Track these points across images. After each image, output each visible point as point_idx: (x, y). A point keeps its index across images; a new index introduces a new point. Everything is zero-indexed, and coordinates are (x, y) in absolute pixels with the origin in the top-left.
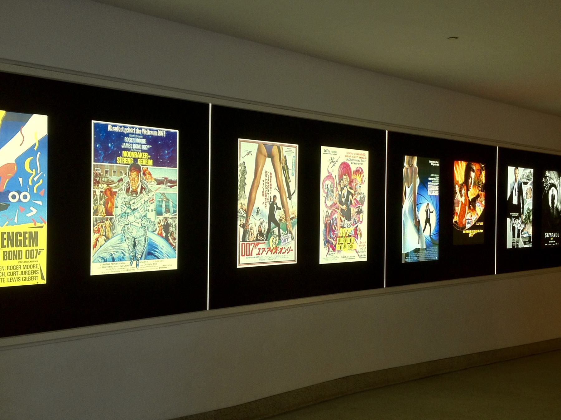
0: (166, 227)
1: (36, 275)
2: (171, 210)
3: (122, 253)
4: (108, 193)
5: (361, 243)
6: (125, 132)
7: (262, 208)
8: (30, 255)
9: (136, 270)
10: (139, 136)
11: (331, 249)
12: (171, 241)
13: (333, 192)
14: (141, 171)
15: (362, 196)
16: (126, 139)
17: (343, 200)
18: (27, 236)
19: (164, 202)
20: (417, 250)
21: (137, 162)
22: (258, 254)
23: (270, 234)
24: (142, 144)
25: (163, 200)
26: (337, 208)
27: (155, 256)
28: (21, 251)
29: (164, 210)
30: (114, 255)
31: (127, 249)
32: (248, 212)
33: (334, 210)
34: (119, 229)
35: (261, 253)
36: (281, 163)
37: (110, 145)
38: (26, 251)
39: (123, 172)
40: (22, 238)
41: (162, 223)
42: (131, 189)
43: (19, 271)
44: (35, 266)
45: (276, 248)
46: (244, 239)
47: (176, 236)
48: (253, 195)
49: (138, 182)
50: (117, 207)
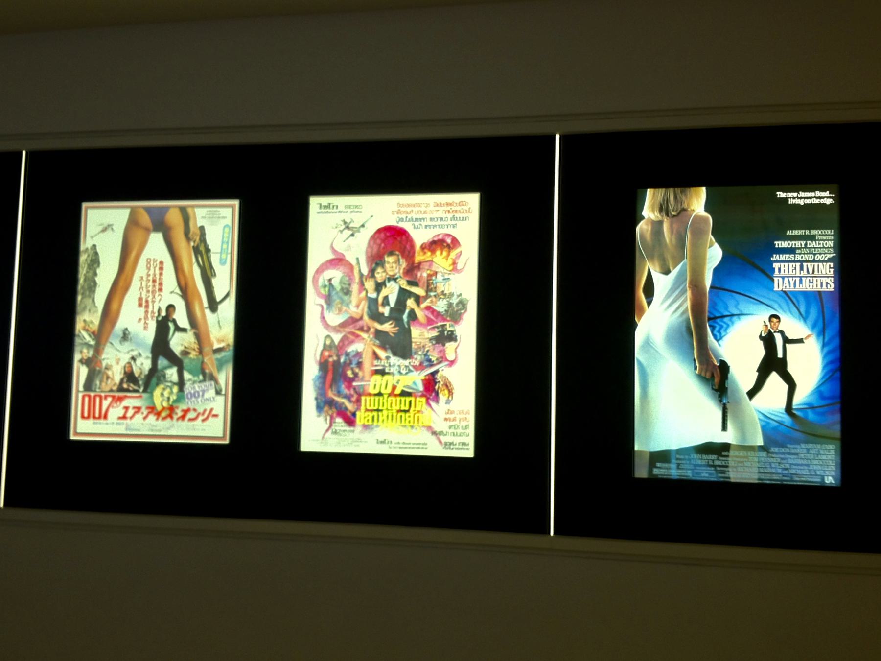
5: (449, 412)
7: (135, 328)
11: (339, 420)
13: (347, 292)
15: (455, 300)
17: (386, 311)
20: (714, 450)
22: (124, 417)
23: (154, 380)
26: (361, 329)
32: (101, 336)
33: (353, 334)
35: (129, 414)
36: (188, 239)
45: (172, 409)
46: (88, 386)
48: (114, 306)
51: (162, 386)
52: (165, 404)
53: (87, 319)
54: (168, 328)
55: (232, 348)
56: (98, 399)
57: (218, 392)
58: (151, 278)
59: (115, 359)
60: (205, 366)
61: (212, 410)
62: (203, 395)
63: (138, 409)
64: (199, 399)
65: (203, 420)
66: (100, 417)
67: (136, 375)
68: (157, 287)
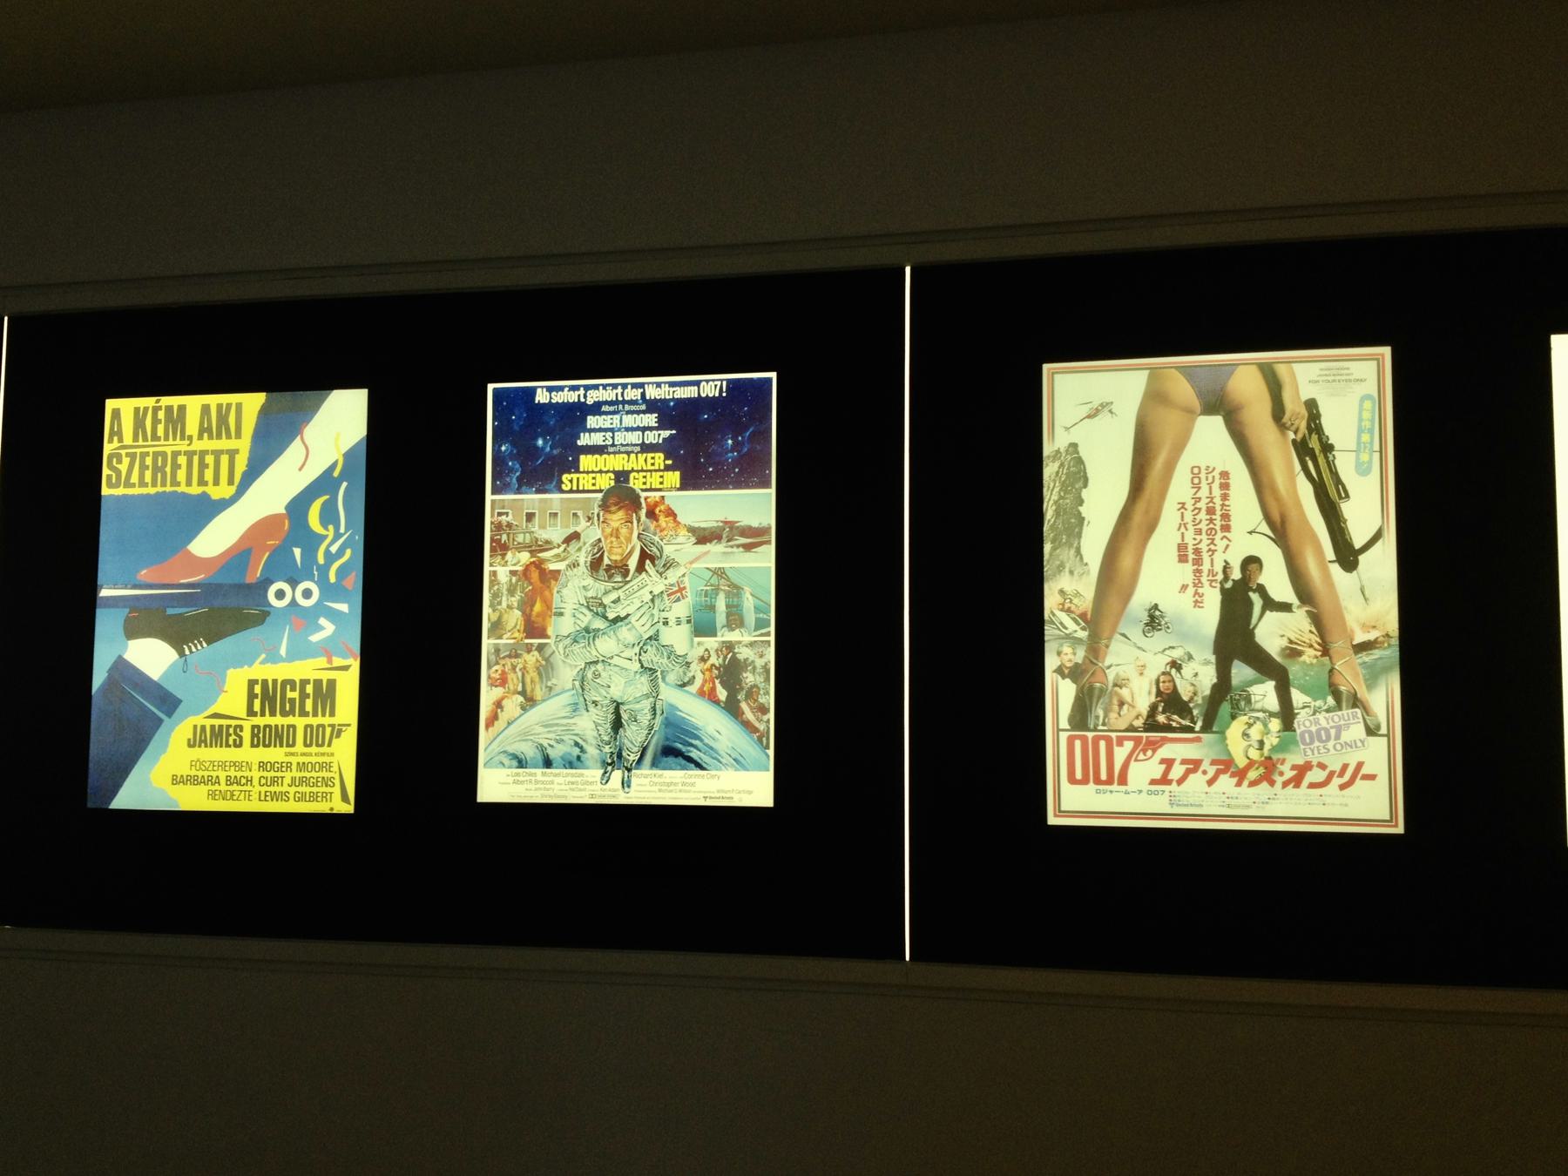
0: (731, 672)
1: (328, 790)
2: (750, 618)
3: (577, 744)
4: (535, 575)
6: (590, 401)
7: (1174, 603)
8: (315, 737)
9: (622, 798)
10: (633, 408)
12: (749, 715)
14: (637, 506)
16: (592, 421)
18: (309, 689)
19: (722, 596)
21: (627, 480)
22: (1164, 780)
23: (1225, 708)
24: (644, 429)
25: (717, 590)
27: (690, 760)
28: (294, 727)
29: (721, 618)
30: (550, 751)
31: (590, 734)
34: (566, 675)
37: (540, 442)
38: (306, 727)
39: (580, 513)
40: (295, 695)
41: (714, 660)
42: (606, 561)
43: (288, 776)
44: (326, 766)
45: (1269, 769)
47: (770, 700)
48: (1126, 561)
49: (629, 540)
50: (561, 614)
51: (1245, 719)
52: (1254, 754)
53: (1068, 588)
54: (1250, 604)
55: (1395, 641)
56: (1102, 744)
57: (1371, 731)
58: (1202, 505)
59: (1135, 667)
60: (1338, 679)
61: (1360, 765)
62: (1338, 737)
63: (1194, 765)
64: (1330, 745)
65: (1343, 787)
66: (1110, 781)
67: (1185, 698)
68: (1218, 523)
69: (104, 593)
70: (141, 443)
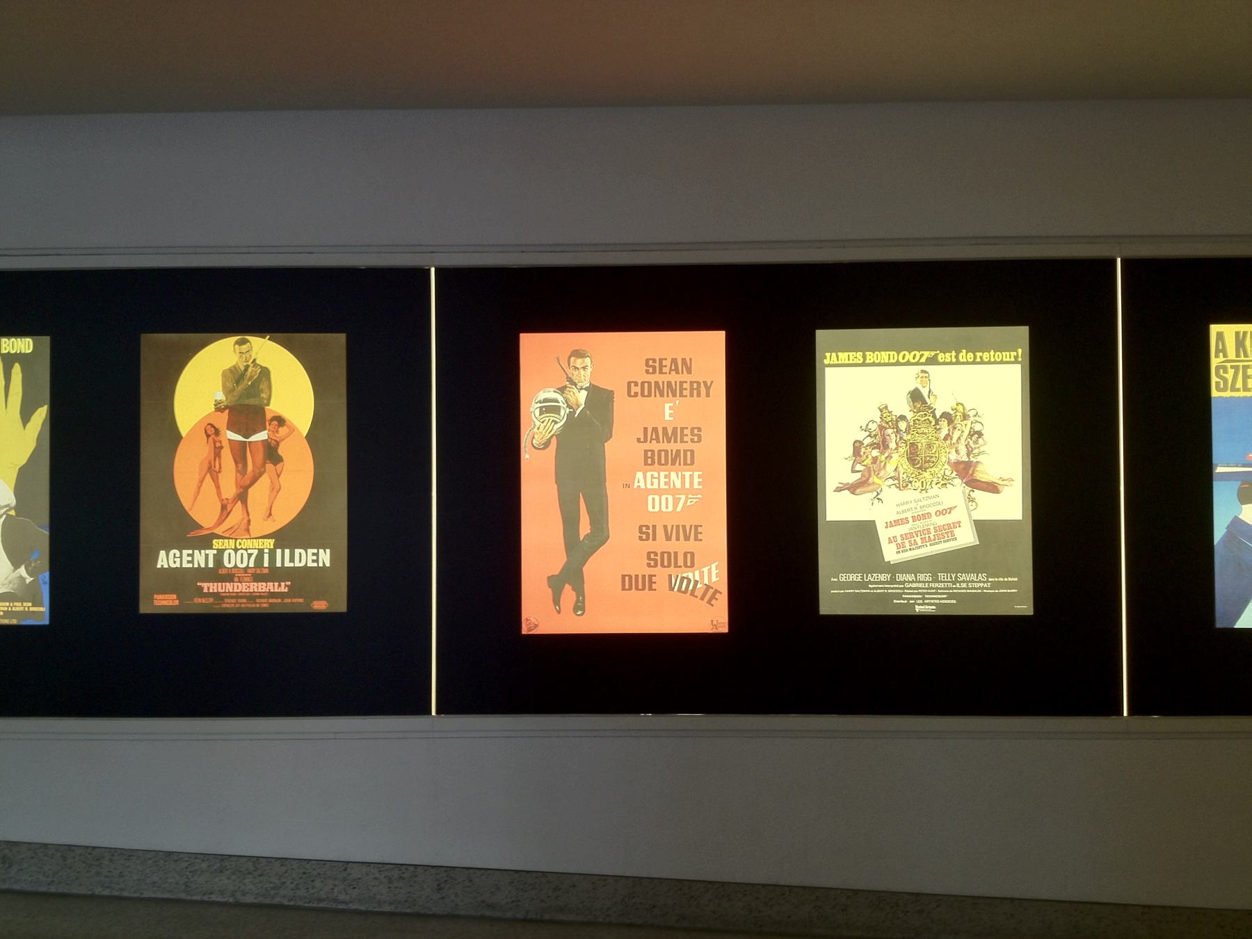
69: (1219, 470)
70: (1242, 358)
